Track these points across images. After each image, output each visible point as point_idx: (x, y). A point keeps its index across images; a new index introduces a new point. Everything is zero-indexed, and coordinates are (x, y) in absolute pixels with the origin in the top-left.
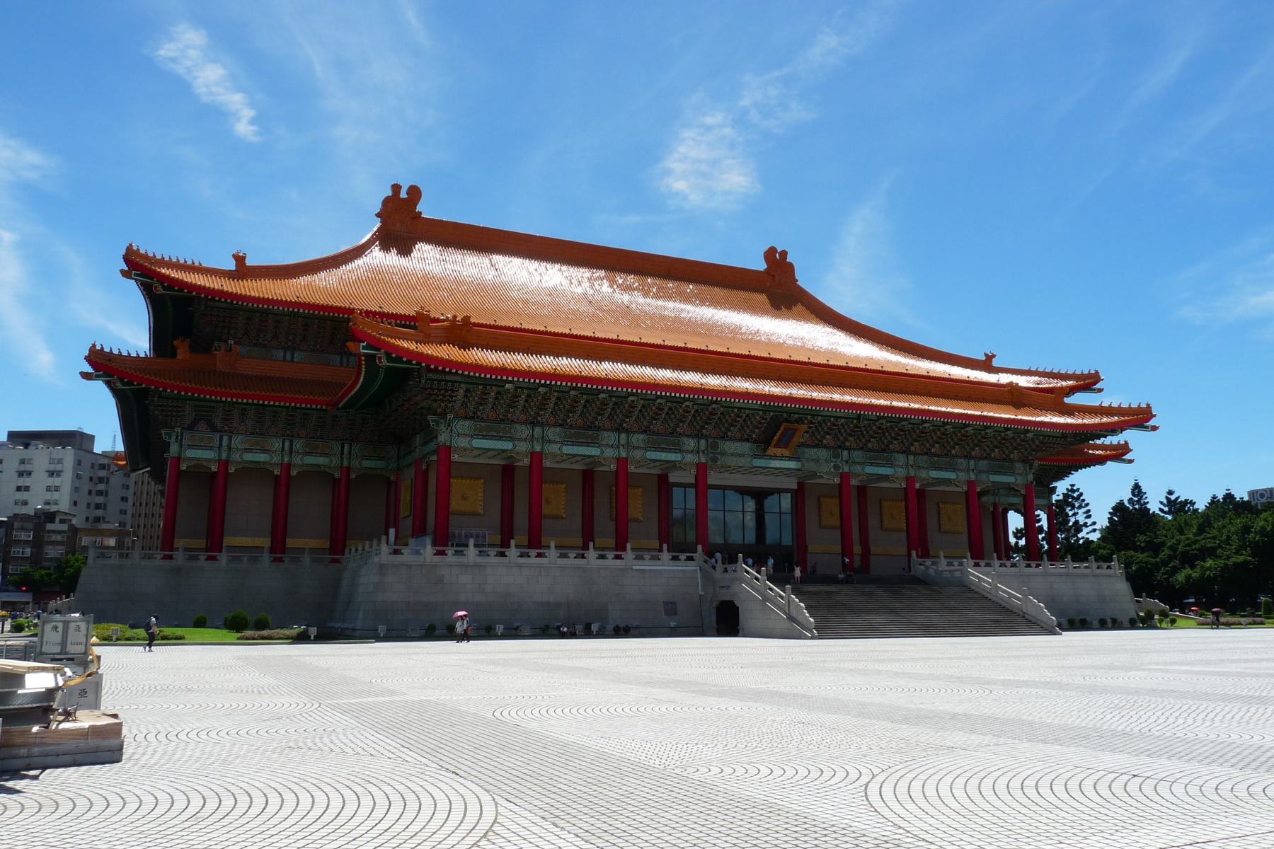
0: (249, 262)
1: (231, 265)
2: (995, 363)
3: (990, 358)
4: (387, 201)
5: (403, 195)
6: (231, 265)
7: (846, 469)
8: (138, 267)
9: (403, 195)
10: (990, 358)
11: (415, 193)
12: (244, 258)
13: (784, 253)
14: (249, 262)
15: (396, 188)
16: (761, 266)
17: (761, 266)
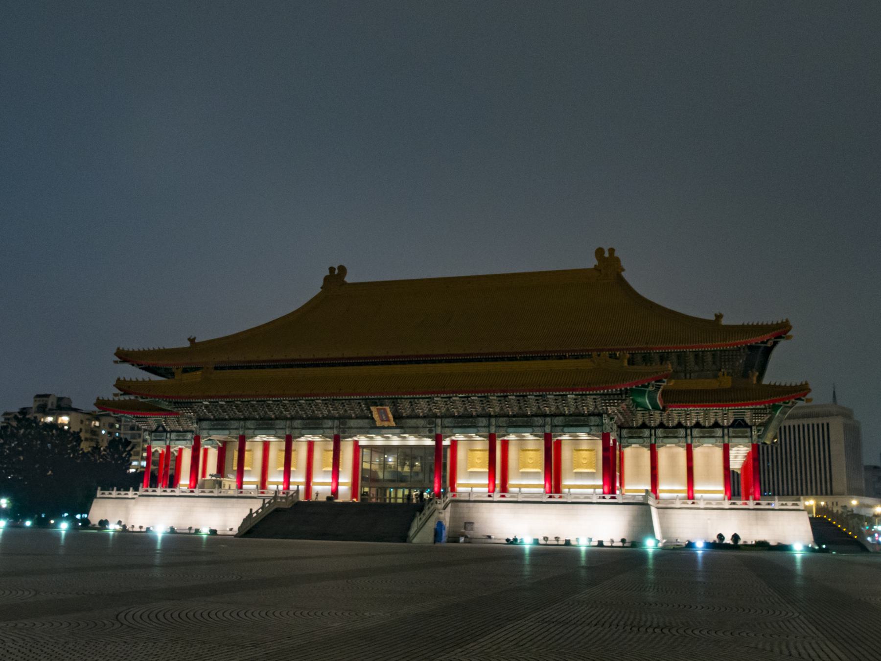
0: (196, 341)
1: (187, 344)
2: (724, 322)
3: (719, 317)
4: (326, 279)
5: (336, 272)
6: (187, 344)
7: (439, 432)
8: (124, 357)
9: (336, 272)
10: (719, 317)
11: (343, 269)
12: (194, 339)
13: (612, 251)
14: (196, 341)
15: (332, 269)
16: (591, 262)
17: (591, 262)
